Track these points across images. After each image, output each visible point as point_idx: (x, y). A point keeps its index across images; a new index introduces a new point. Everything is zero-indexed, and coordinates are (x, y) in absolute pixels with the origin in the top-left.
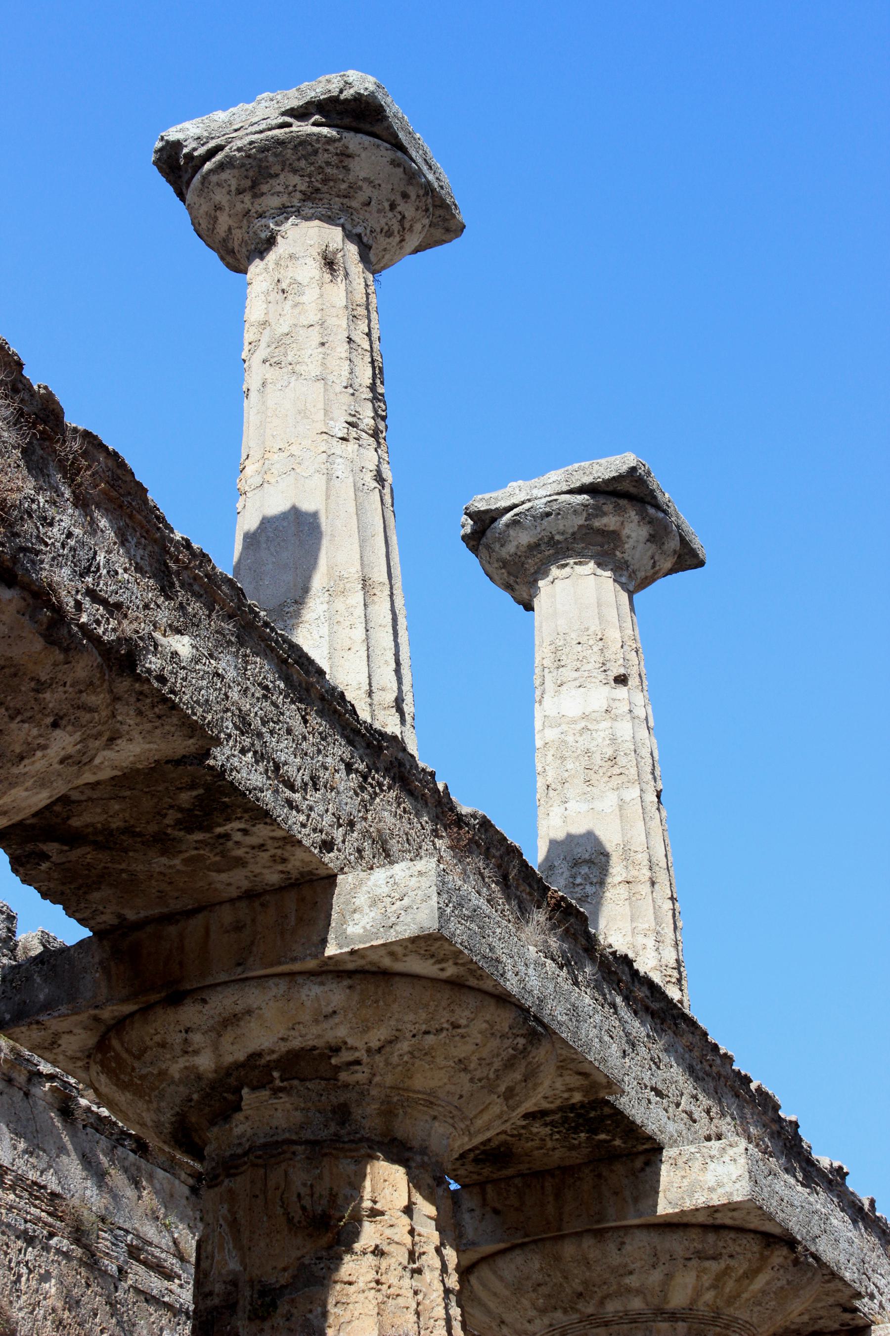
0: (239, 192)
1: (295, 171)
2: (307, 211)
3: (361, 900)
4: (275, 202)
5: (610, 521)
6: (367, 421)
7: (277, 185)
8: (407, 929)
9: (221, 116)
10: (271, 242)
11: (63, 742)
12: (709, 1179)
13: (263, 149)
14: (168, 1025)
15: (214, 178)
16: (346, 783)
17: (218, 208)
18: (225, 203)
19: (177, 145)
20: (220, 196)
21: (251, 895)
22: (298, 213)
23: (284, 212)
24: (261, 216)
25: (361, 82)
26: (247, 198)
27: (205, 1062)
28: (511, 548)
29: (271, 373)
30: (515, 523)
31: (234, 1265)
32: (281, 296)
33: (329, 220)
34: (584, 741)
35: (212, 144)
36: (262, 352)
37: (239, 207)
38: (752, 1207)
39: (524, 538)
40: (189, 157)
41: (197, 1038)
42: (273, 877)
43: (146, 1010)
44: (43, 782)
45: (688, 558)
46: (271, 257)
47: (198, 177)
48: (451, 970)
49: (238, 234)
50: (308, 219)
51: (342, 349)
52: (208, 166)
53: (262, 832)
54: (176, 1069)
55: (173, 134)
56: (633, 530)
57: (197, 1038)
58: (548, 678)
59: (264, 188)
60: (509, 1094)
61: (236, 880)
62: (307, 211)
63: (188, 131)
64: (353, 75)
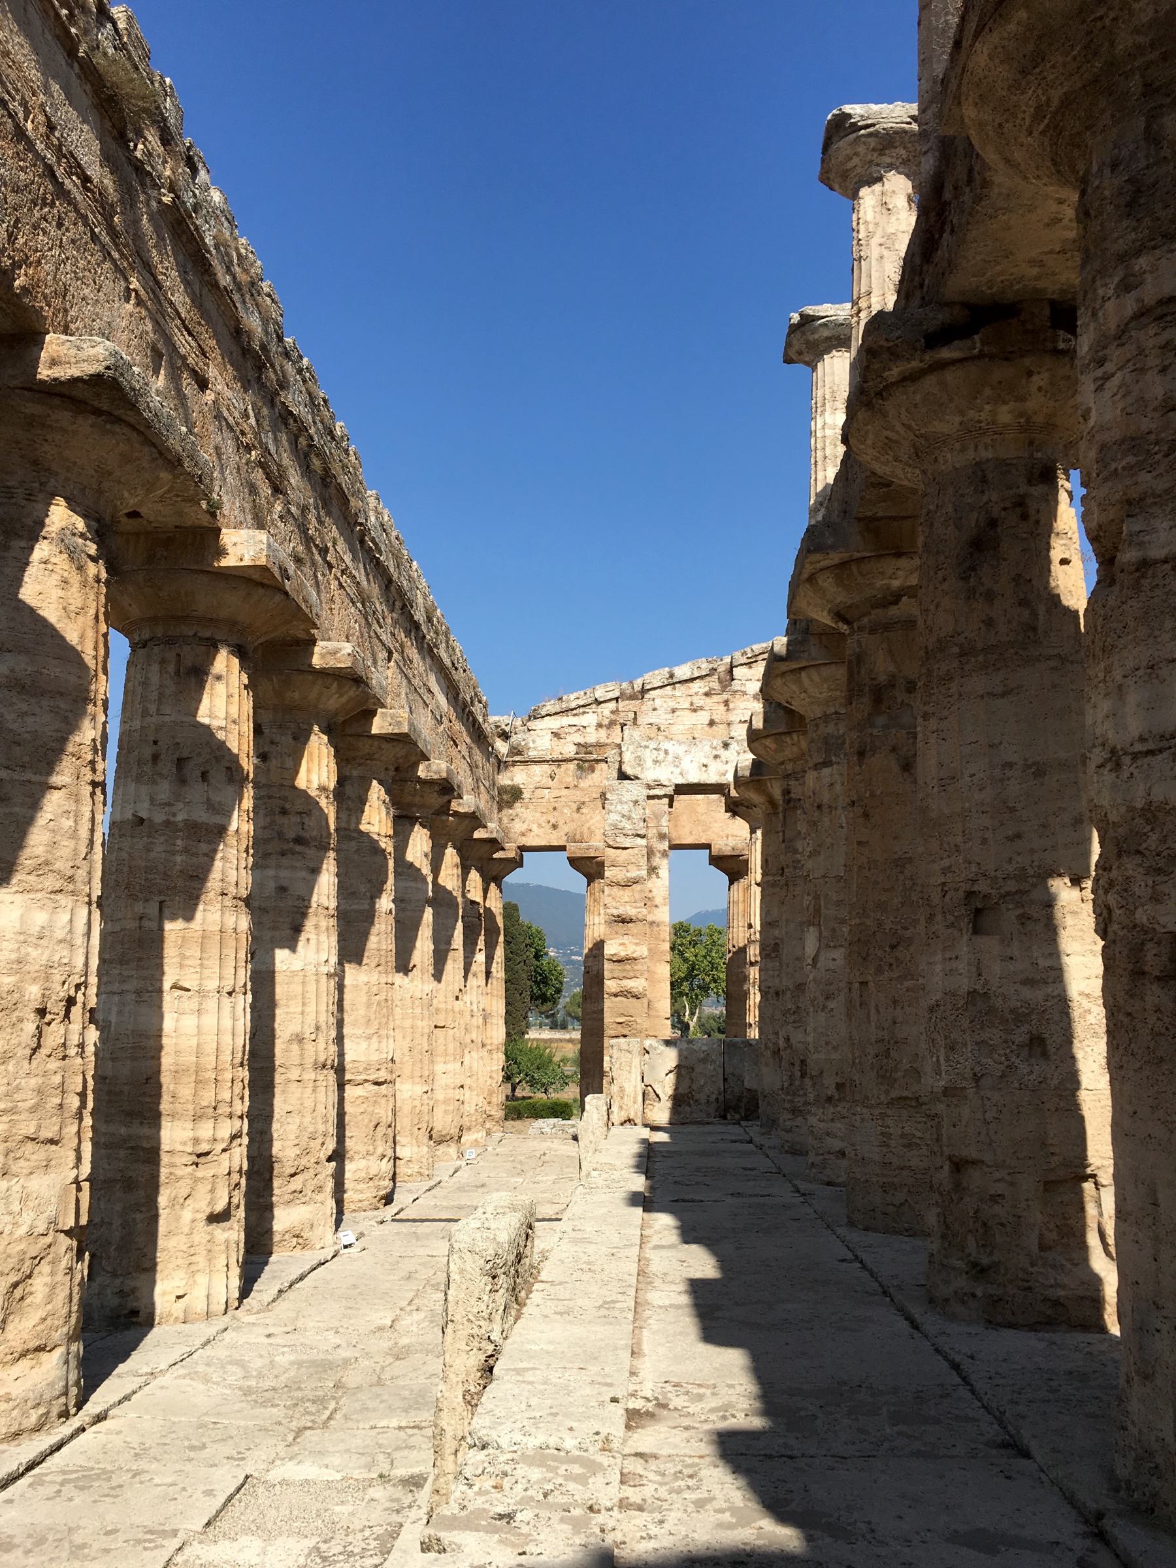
0: (873, 150)
1: (905, 148)
2: (901, 170)
4: (888, 160)
7: (894, 152)
9: (875, 107)
10: (880, 179)
13: (896, 133)
14: (889, 565)
15: (863, 139)
17: (856, 154)
18: (862, 154)
19: (850, 116)
20: (861, 149)
22: (897, 169)
23: (890, 167)
24: (878, 165)
26: (876, 154)
28: (816, 336)
29: (886, 253)
30: (825, 325)
31: (892, 669)
32: (884, 211)
33: (908, 176)
35: (869, 122)
36: (875, 241)
37: (869, 157)
39: (826, 333)
40: (855, 124)
43: (879, 556)
46: (877, 187)
47: (853, 136)
49: (859, 170)
50: (900, 173)
52: (863, 132)
55: (847, 109)
57: (900, 573)
58: (827, 405)
59: (887, 152)
62: (901, 170)
63: (856, 110)
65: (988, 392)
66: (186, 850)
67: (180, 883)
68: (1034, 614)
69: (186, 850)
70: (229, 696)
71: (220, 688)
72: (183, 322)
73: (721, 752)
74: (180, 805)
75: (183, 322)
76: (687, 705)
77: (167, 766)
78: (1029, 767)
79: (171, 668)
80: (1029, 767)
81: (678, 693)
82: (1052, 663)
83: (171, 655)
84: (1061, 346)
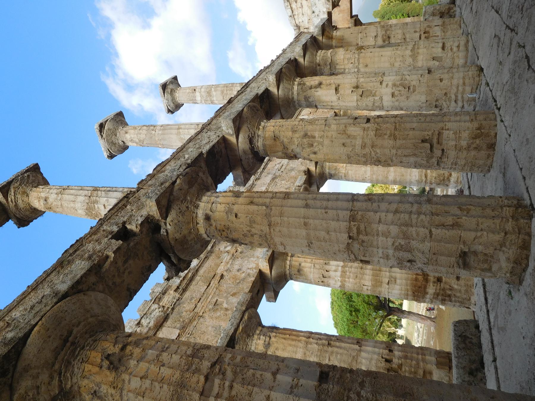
3: (227, 131)
5: (169, 90)
6: (152, 128)
7: (114, 140)
8: (232, 124)
11: (201, 174)
12: (272, 80)
16: (209, 133)
21: (226, 148)
25: (96, 126)
27: (251, 156)
34: (205, 96)
38: (276, 75)
41: (247, 157)
42: (223, 145)
44: (207, 178)
45: (175, 78)
48: (238, 118)
51: (141, 131)
53: (216, 146)
54: (252, 161)
56: (170, 87)
60: (257, 110)
61: (224, 150)
63: (105, 154)
64: (95, 127)
65: (185, 246)
66: (349, 278)
67: (358, 280)
68: (255, 234)
69: (349, 278)
70: (305, 261)
71: (303, 264)
72: (208, 287)
73: (316, 13)
74: (336, 278)
75: (208, 287)
76: (301, 9)
77: (325, 280)
78: (309, 245)
79: (298, 276)
80: (309, 245)
81: (297, 13)
82: (272, 231)
83: (295, 276)
84: (165, 234)
